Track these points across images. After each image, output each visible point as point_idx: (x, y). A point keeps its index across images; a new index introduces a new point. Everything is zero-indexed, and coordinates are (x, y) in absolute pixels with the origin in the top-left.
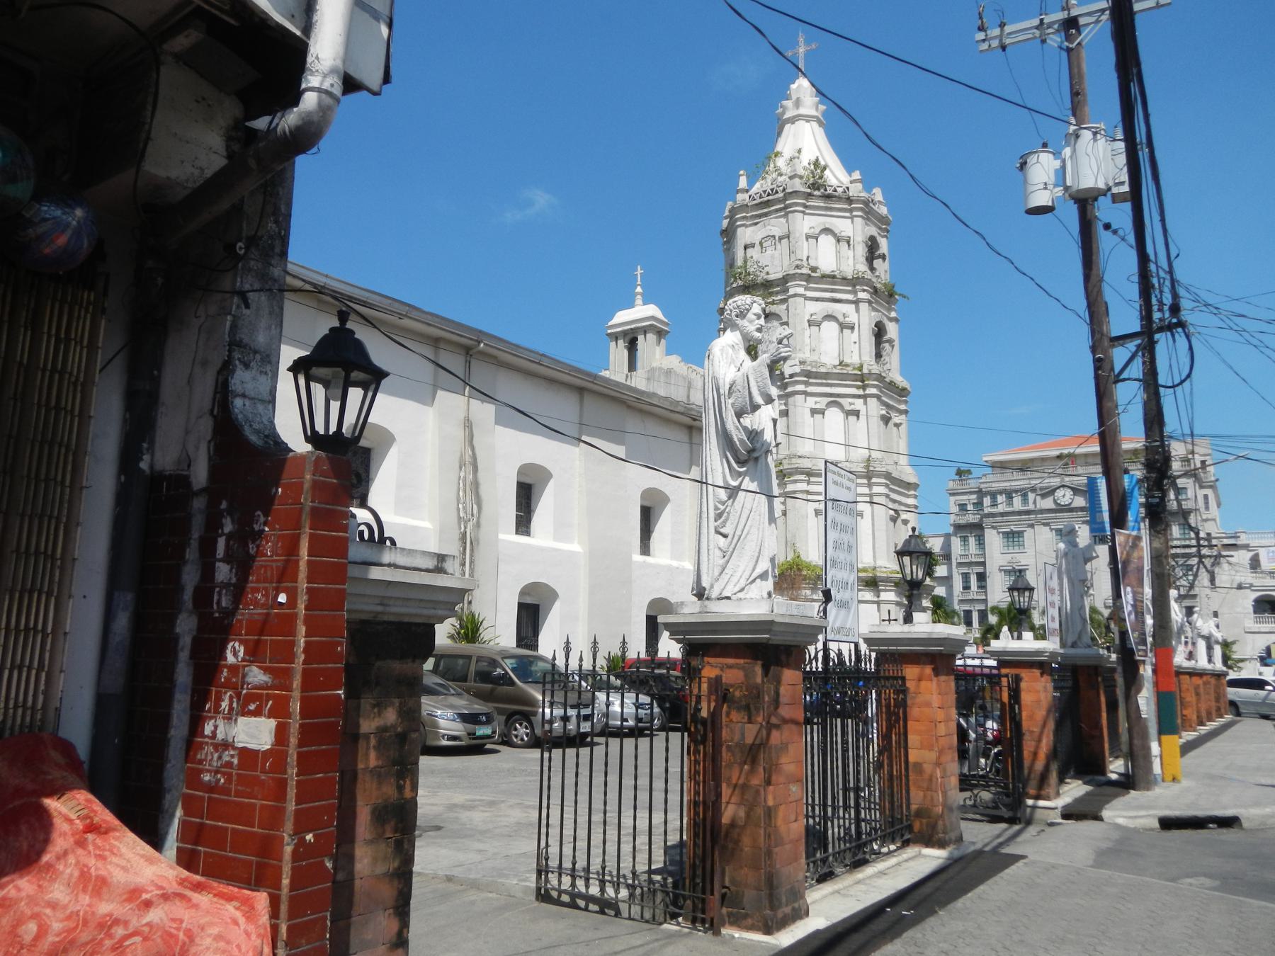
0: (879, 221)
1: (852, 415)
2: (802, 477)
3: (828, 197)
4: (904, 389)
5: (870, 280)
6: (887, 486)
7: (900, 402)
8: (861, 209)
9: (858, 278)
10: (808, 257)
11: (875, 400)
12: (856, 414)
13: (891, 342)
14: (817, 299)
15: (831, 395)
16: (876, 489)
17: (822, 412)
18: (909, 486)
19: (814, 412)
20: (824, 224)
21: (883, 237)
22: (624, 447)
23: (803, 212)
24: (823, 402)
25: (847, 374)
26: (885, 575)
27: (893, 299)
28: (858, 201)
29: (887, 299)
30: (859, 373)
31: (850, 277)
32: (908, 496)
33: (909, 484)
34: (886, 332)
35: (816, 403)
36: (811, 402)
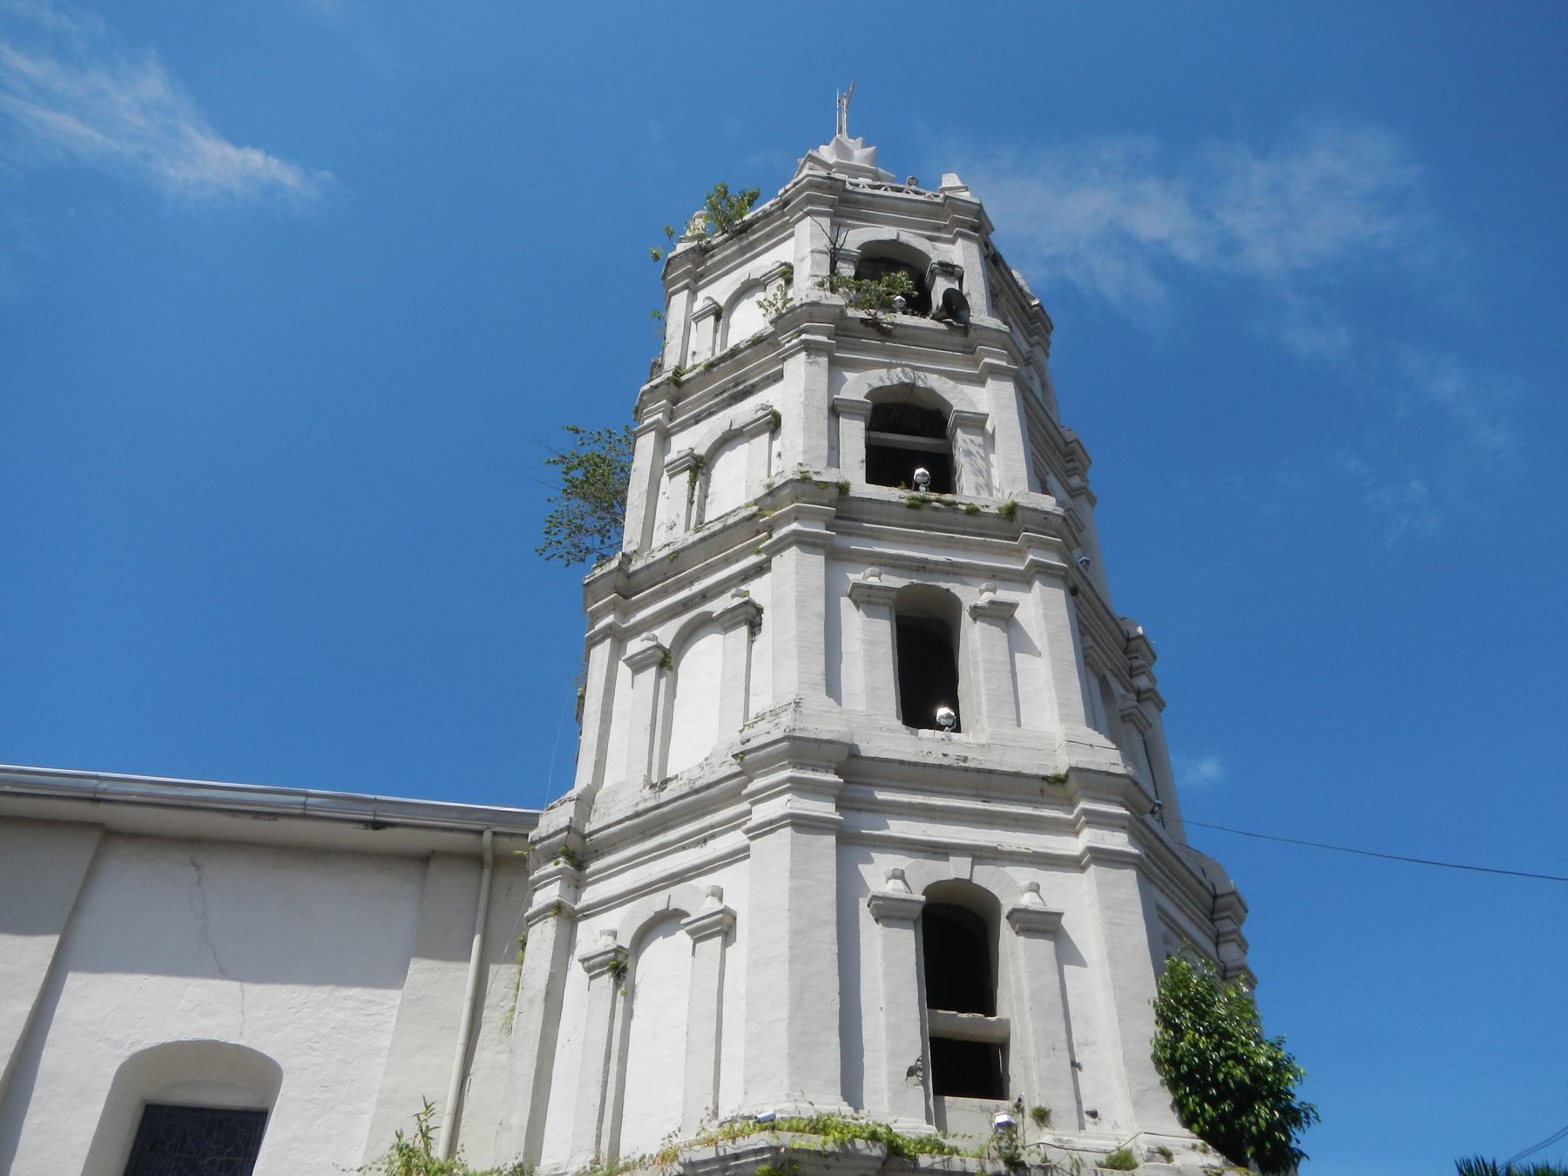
0: (928, 215)
1: (735, 626)
2: (551, 867)
3: (746, 228)
4: (1011, 511)
5: (813, 304)
6: (799, 787)
7: (1019, 553)
8: (810, 200)
9: (781, 316)
10: (694, 353)
11: (793, 552)
12: (751, 617)
13: (976, 423)
14: (697, 420)
15: (686, 605)
16: (764, 812)
17: (665, 661)
18: (1054, 787)
19: (637, 666)
20: (738, 279)
21: (953, 242)
22: (52, 941)
23: (686, 287)
24: (666, 634)
25: (725, 529)
26: (709, 1153)
27: (972, 333)
28: (799, 192)
29: (957, 339)
30: (755, 509)
31: (771, 329)
32: (1071, 829)
33: (1059, 780)
34: (951, 407)
35: (642, 641)
36: (635, 646)
